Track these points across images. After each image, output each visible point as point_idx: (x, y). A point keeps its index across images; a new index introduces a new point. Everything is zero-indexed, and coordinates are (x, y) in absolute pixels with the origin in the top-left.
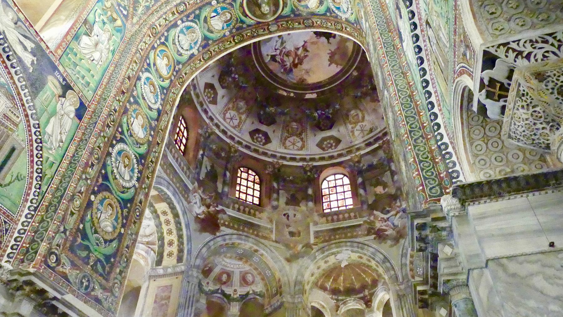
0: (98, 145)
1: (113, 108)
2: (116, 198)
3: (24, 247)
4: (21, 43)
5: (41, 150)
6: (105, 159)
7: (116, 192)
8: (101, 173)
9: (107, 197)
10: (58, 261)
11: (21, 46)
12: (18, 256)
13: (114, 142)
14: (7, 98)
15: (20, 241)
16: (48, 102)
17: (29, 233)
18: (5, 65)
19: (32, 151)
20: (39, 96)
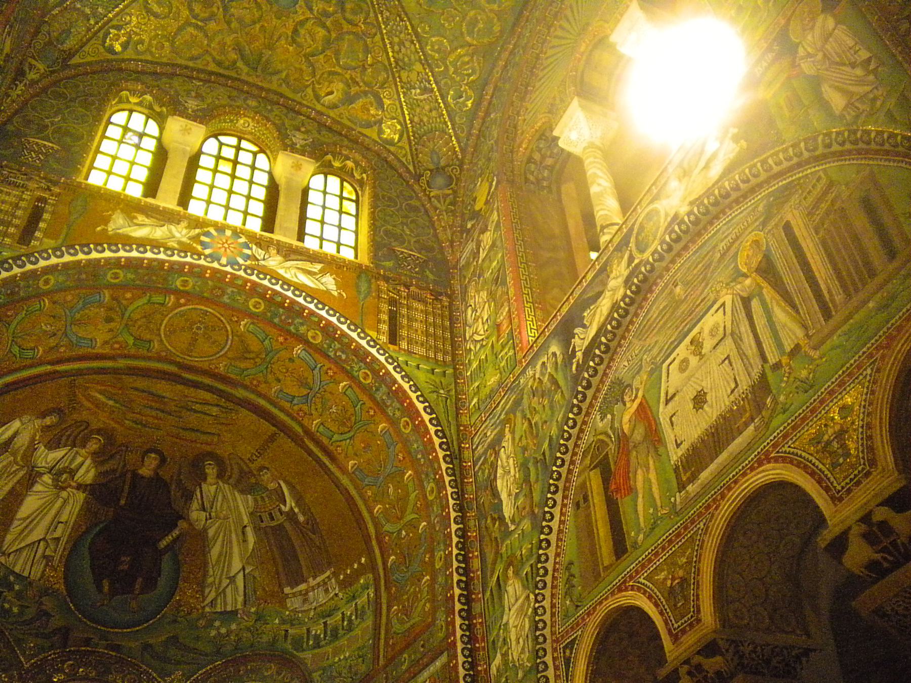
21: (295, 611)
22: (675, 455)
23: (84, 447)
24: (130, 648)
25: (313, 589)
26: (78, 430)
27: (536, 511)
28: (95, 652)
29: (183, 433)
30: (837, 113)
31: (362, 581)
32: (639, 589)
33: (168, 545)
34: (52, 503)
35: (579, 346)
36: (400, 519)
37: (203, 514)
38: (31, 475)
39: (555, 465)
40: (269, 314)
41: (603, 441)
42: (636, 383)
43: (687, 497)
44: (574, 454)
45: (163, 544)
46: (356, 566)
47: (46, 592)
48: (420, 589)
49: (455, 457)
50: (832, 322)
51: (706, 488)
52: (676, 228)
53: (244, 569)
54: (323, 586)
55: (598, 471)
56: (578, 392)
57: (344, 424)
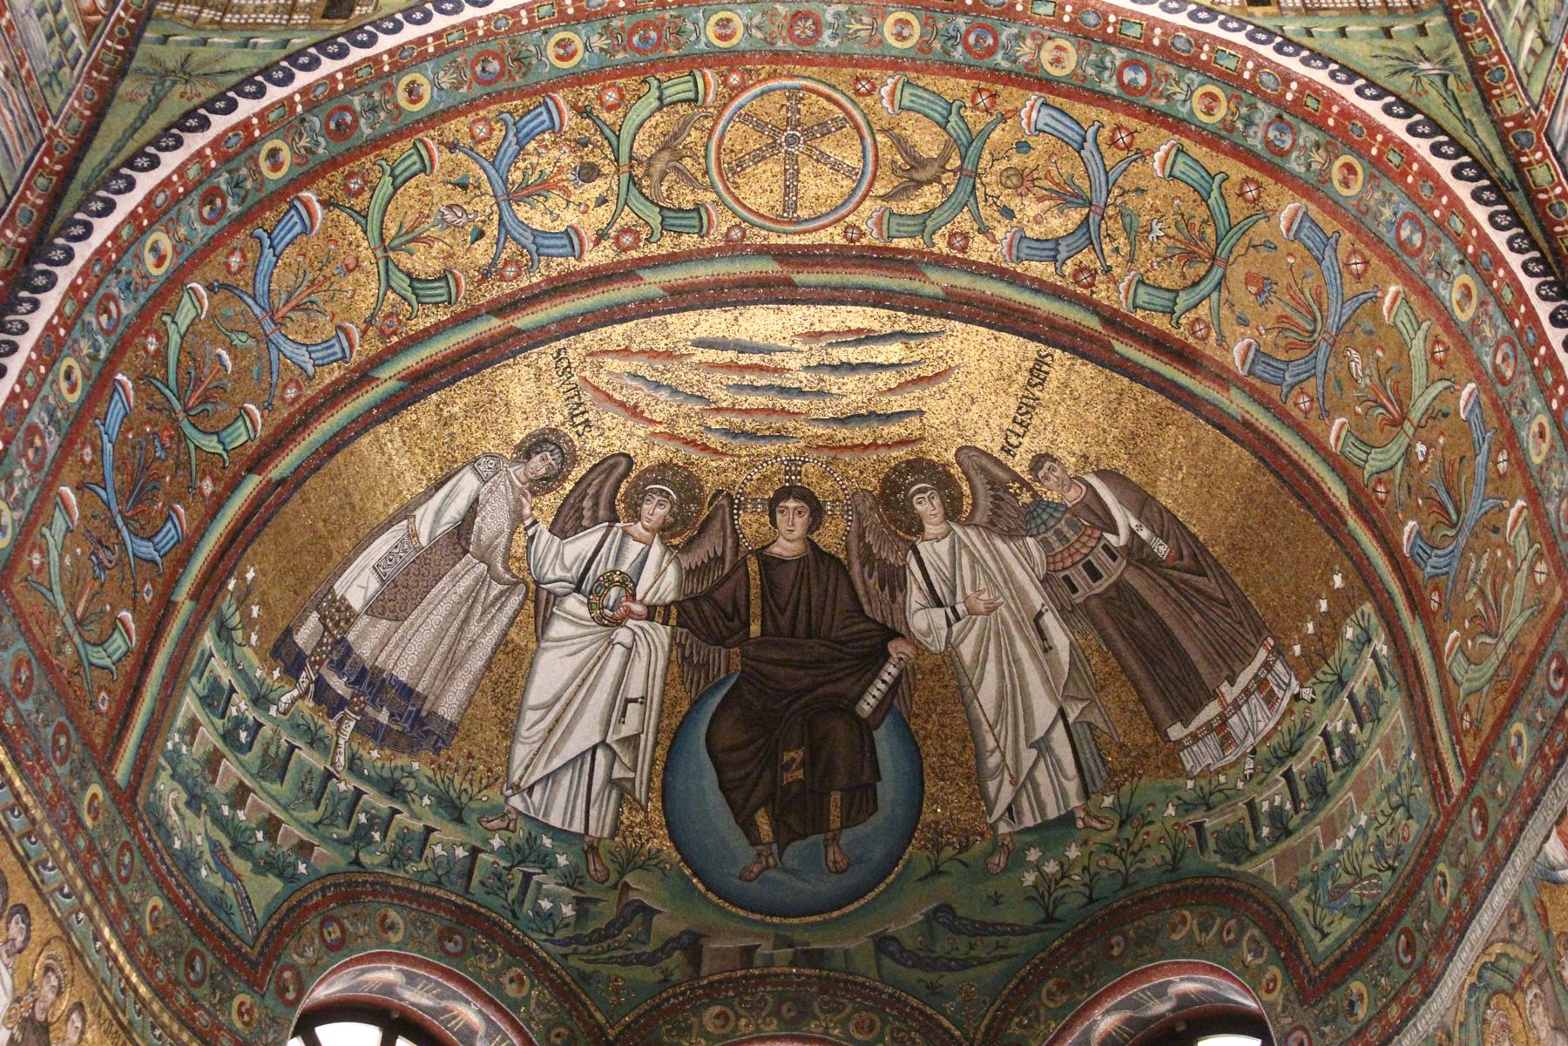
21: (1207, 772)
23: (636, 517)
24: (846, 952)
25: (1237, 707)
26: (612, 480)
28: (769, 975)
29: (842, 433)
31: (1350, 633)
33: (881, 702)
34: (600, 660)
36: (1397, 423)
37: (938, 615)
38: (536, 602)
40: (937, 45)
45: (867, 706)
46: (1324, 605)
47: (630, 861)
48: (1505, 546)
53: (1062, 713)
54: (1260, 689)
57: (1190, 257)
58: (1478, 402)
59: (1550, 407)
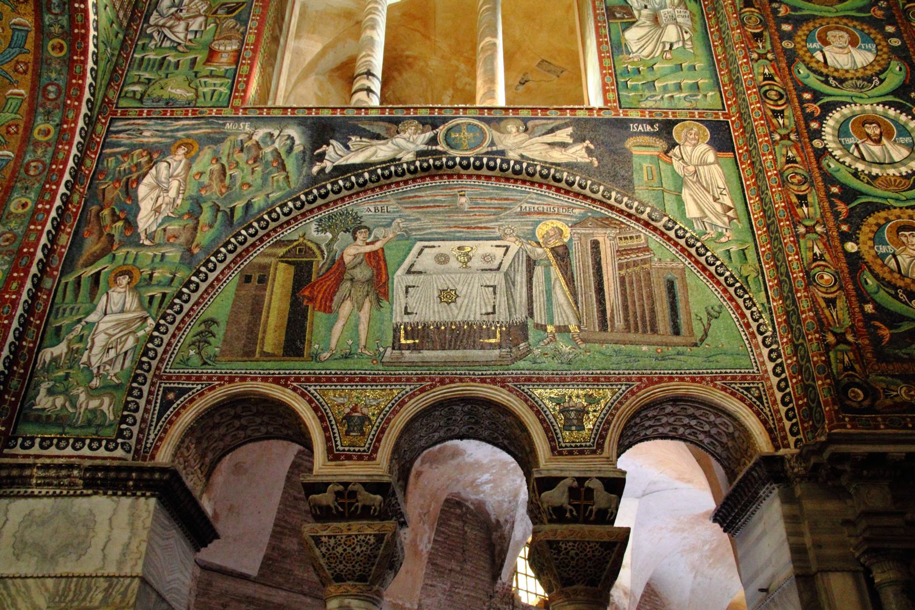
0: (784, 160)
1: (761, 78)
2: (907, 208)
3: (802, 405)
4: (552, 145)
5: (707, 250)
6: (820, 168)
7: (897, 200)
8: (834, 195)
9: (882, 222)
10: (870, 392)
11: (557, 148)
12: (806, 425)
13: (814, 125)
14: (601, 227)
15: (791, 401)
16: (656, 179)
17: (794, 381)
18: (562, 191)
19: (697, 262)
20: (636, 182)
22: (399, 317)
27: (196, 251)
30: (688, 216)
32: (303, 395)
35: (330, 156)
39: (246, 229)
41: (310, 249)
42: (378, 232)
43: (398, 358)
44: (268, 235)
49: (91, 121)
50: (604, 335)
51: (425, 363)
52: (499, 161)
55: (292, 269)
56: (311, 192)
58: (8, 162)
59: (37, 204)
